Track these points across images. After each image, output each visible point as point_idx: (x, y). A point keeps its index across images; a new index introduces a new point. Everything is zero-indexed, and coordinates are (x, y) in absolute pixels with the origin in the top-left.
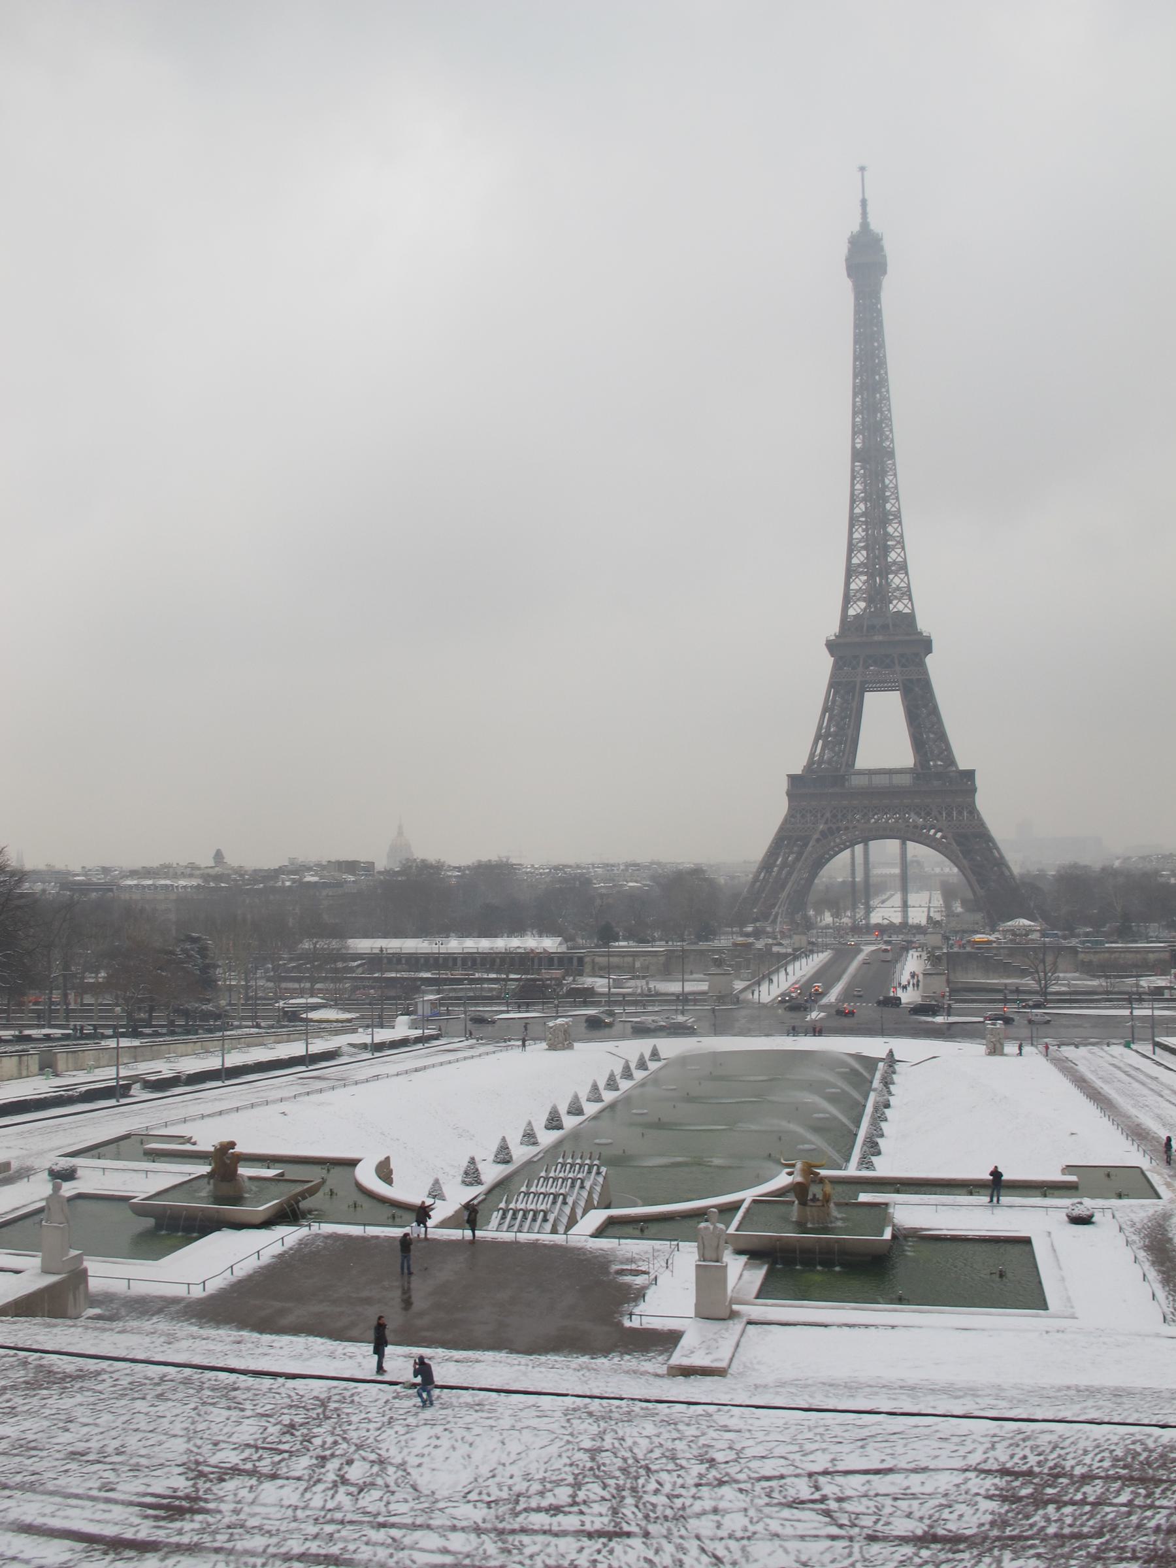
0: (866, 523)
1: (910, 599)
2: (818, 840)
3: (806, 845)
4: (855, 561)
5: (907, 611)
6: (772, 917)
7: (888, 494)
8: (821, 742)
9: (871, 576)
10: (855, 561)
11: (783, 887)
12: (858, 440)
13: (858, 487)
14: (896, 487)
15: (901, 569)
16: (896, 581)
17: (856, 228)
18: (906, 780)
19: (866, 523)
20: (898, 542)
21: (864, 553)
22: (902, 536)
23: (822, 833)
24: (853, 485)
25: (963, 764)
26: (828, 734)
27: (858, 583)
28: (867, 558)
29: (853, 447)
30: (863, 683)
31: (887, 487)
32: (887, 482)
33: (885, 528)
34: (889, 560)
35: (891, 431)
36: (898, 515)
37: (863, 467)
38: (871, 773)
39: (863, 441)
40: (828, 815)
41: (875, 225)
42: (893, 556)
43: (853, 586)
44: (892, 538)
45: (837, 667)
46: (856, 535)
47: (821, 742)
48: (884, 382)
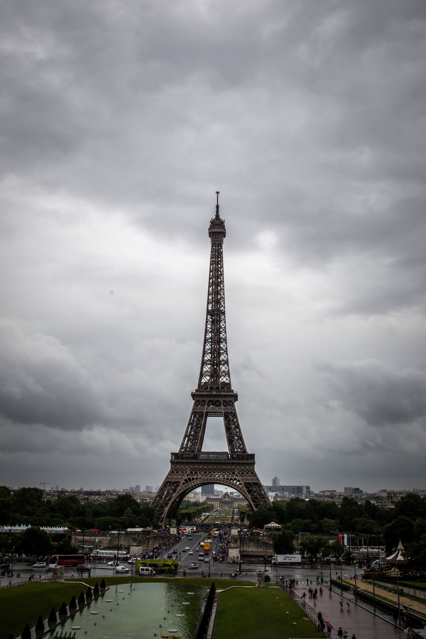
0: (211, 342)
1: (229, 377)
2: (184, 484)
3: (178, 486)
5: (227, 382)
6: (161, 519)
7: (221, 330)
8: (187, 438)
9: (213, 365)
10: (206, 358)
11: (166, 505)
12: (209, 306)
13: (209, 326)
14: (225, 327)
15: (226, 363)
16: (223, 368)
17: (214, 217)
18: (225, 457)
19: (211, 342)
20: (225, 351)
21: (210, 355)
22: (227, 349)
24: (206, 325)
25: (249, 451)
26: (190, 435)
27: (207, 368)
28: (211, 358)
29: (208, 309)
30: (207, 413)
31: (221, 327)
32: (221, 325)
33: (219, 345)
34: (221, 359)
35: (224, 303)
36: (225, 340)
37: (211, 318)
39: (212, 308)
40: (189, 472)
42: (222, 357)
43: (204, 369)
44: (223, 350)
45: (196, 405)
47: (187, 438)
48: (222, 282)
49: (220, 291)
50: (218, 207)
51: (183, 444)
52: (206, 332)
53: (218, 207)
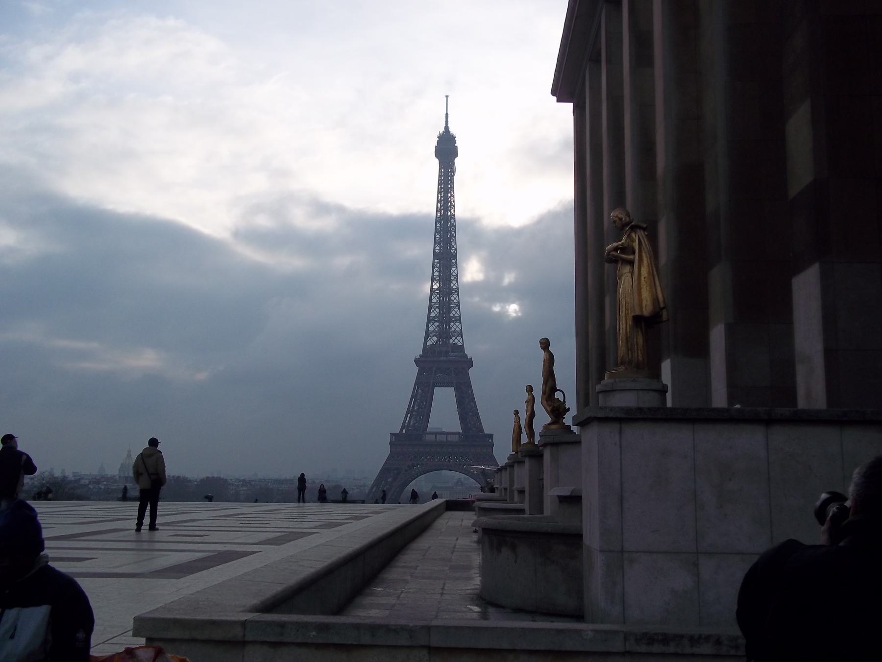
0: (439, 293)
2: (406, 471)
4: (433, 315)
5: (459, 344)
10: (433, 315)
15: (456, 321)
16: (455, 327)
18: (455, 438)
19: (439, 293)
23: (409, 466)
24: (433, 273)
33: (450, 298)
36: (457, 291)
38: (436, 434)
41: (452, 130)
43: (431, 329)
45: (420, 374)
46: (434, 301)
49: (451, 227)
50: (447, 114)
51: (404, 422)
52: (432, 281)
53: (447, 114)
